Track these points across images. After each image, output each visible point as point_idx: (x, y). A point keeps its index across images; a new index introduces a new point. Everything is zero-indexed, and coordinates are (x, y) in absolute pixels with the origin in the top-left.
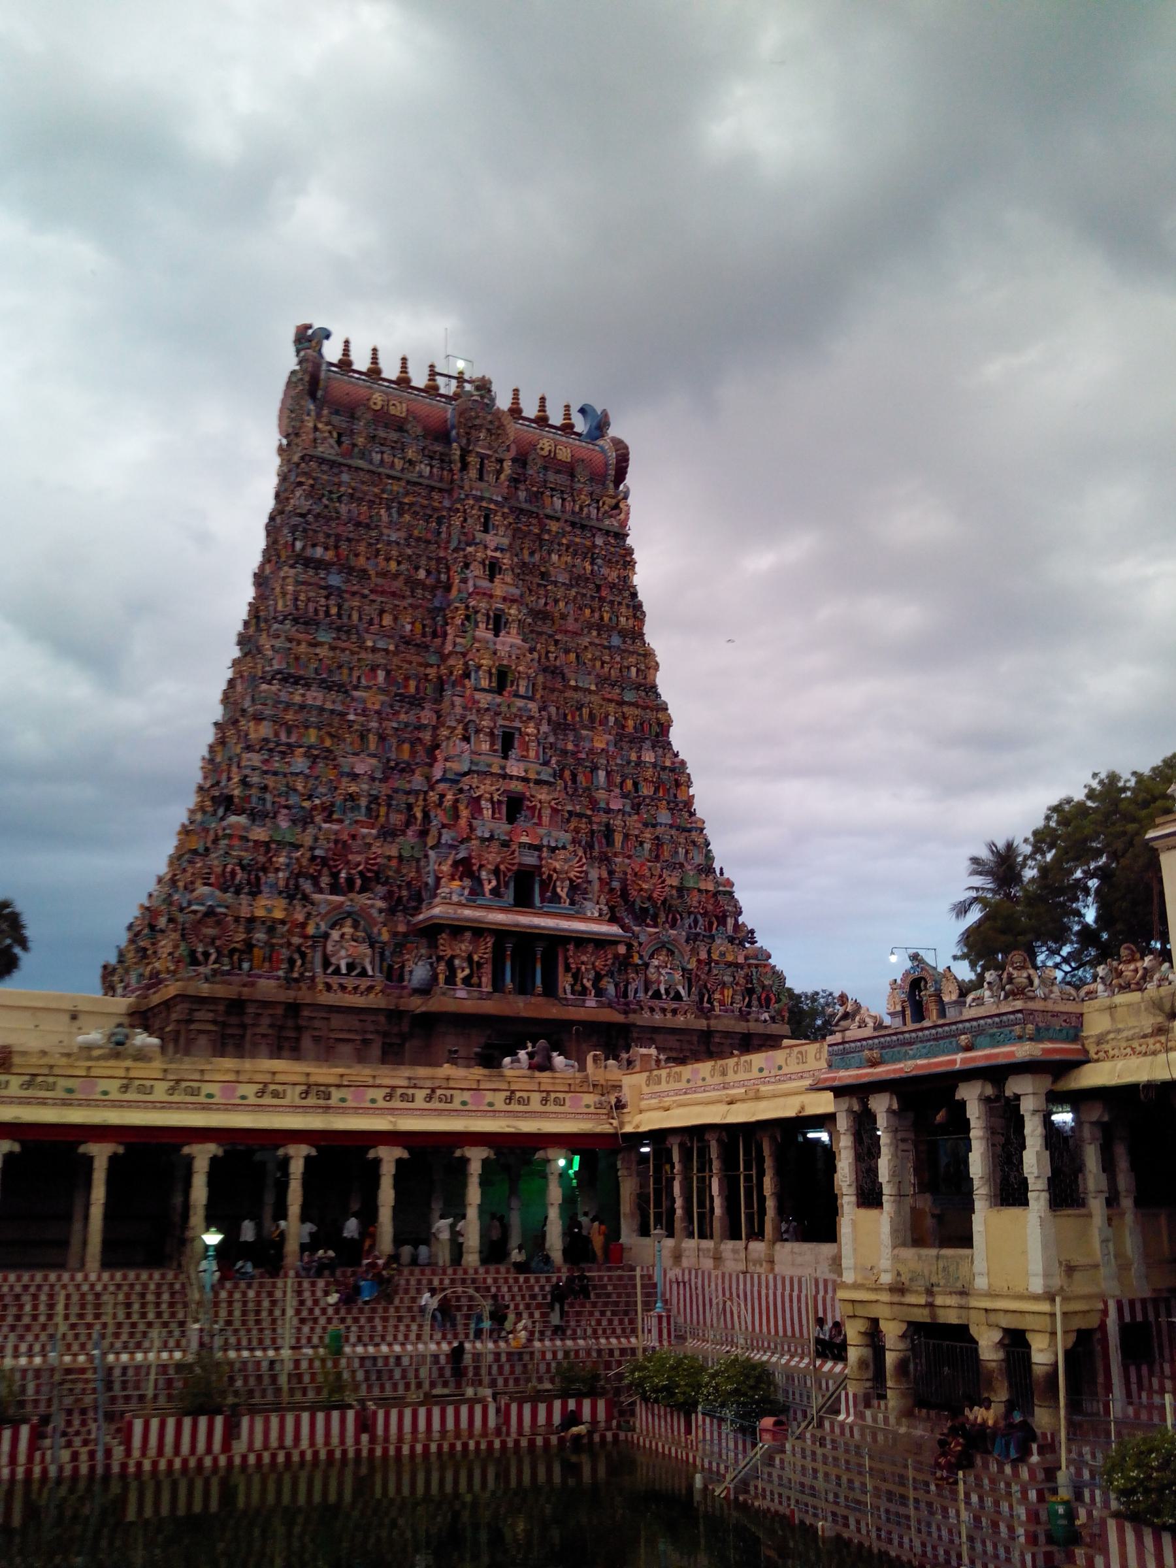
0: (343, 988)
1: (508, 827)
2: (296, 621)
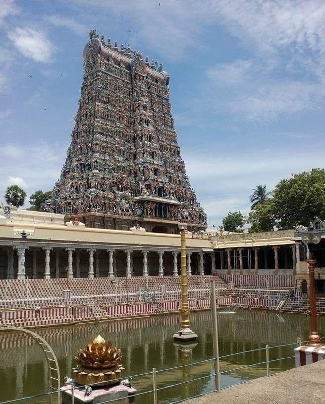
0: (124, 214)
1: (156, 177)
2: (101, 118)
